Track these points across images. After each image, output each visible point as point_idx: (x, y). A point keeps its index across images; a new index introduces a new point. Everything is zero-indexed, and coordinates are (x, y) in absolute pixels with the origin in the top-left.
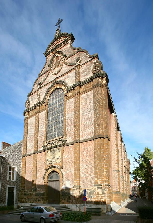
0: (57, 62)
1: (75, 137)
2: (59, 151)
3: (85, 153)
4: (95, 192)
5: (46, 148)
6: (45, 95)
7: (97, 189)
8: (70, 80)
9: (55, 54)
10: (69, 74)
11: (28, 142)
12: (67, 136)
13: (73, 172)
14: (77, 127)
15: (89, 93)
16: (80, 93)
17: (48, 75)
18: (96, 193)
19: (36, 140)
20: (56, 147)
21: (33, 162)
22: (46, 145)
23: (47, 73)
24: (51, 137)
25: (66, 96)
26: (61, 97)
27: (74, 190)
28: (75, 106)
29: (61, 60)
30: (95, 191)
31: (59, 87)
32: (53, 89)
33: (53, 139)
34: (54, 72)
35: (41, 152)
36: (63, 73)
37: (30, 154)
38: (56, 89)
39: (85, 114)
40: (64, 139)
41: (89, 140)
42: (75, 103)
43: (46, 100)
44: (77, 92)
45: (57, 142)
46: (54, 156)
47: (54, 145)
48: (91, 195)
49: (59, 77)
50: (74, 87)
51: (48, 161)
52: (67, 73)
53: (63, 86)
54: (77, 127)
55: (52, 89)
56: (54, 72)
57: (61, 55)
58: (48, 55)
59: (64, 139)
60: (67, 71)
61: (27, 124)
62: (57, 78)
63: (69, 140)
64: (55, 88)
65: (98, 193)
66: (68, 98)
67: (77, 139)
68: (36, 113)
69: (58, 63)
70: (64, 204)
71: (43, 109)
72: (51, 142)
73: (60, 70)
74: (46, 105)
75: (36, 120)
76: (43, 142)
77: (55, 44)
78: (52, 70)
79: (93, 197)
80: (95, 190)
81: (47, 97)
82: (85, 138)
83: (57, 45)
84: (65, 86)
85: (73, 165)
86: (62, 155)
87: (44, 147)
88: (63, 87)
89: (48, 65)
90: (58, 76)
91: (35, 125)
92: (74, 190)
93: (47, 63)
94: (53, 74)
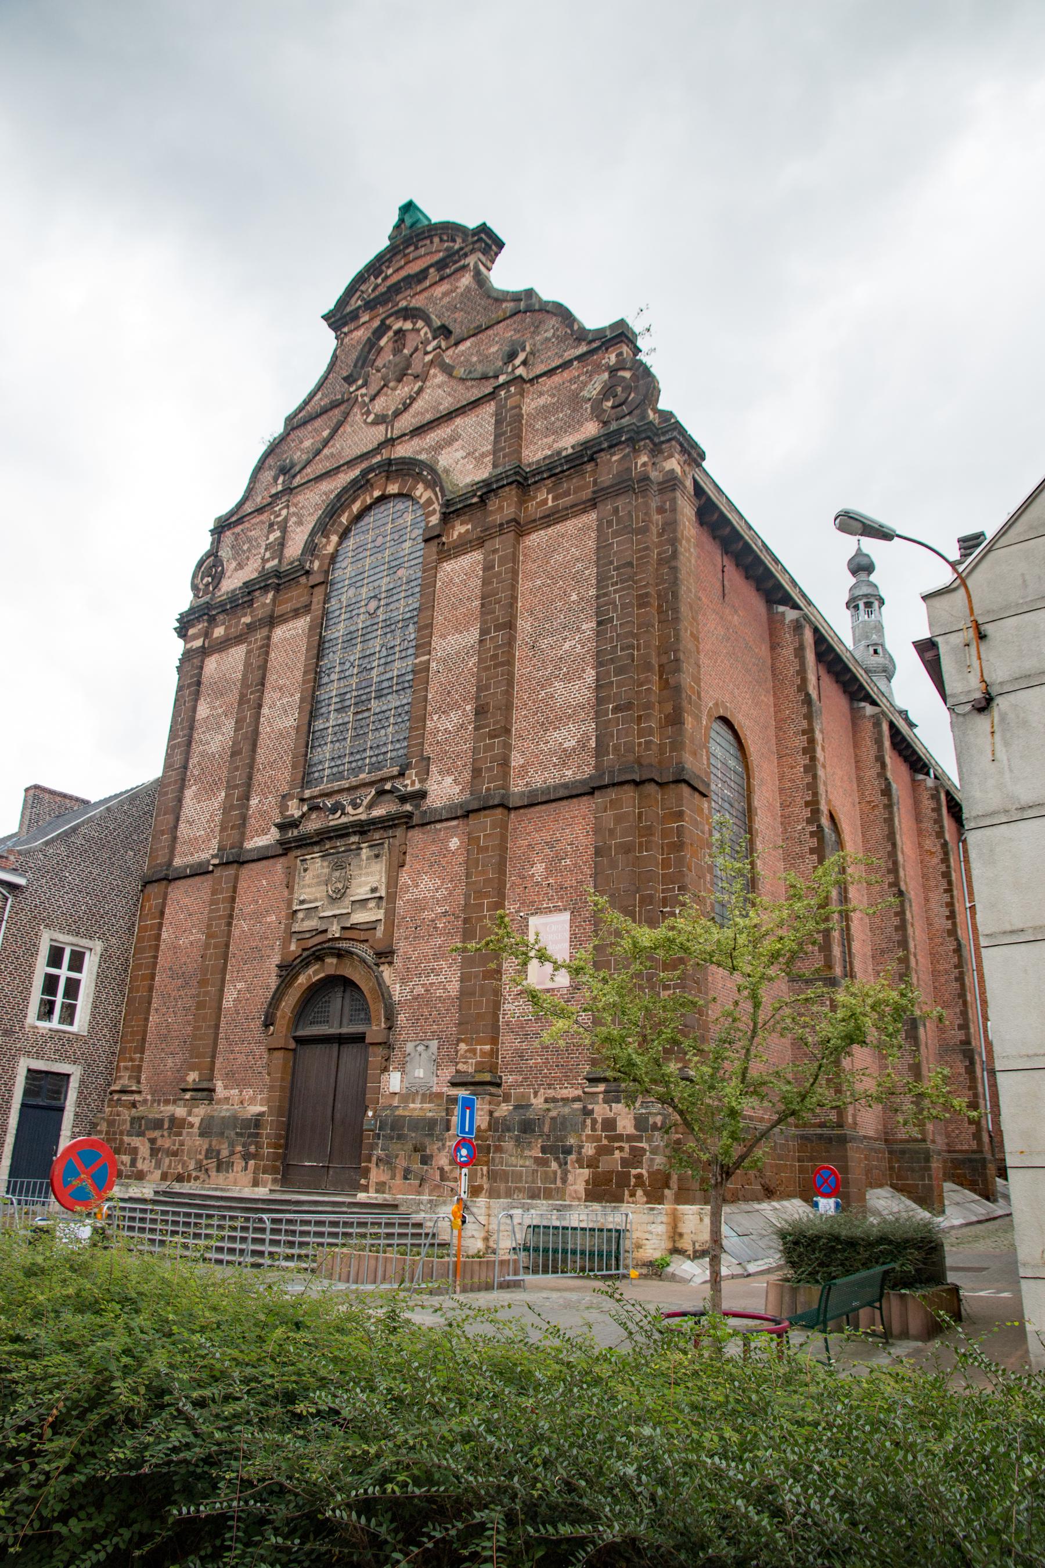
0: (397, 359)
1: (476, 772)
2: (377, 856)
3: (539, 869)
4: (594, 1121)
5: (296, 832)
6: (313, 534)
7: (605, 1102)
8: (461, 453)
9: (388, 322)
10: (458, 421)
11: (189, 793)
12: (433, 768)
13: (454, 987)
14: (493, 716)
15: (570, 526)
16: (520, 528)
17: (340, 424)
18: (599, 1126)
19: (236, 787)
21: (210, 919)
22: (297, 814)
23: (336, 411)
24: (335, 770)
25: (436, 541)
26: (408, 544)
28: (483, 598)
29: (416, 349)
30: (592, 1112)
31: (396, 491)
32: (365, 500)
33: (344, 784)
34: (379, 406)
35: (263, 856)
36: (429, 417)
37: (191, 866)
38: (383, 498)
39: (544, 643)
40: (413, 783)
42: (486, 582)
43: (317, 557)
44: (498, 518)
45: (365, 803)
46: (340, 886)
47: (344, 820)
48: (563, 1139)
49: (404, 435)
50: (487, 490)
51: (300, 915)
52: (449, 416)
53: (420, 487)
54: (493, 716)
55: (354, 501)
56: (379, 406)
57: (420, 324)
58: (345, 324)
59: (408, 782)
60: (447, 404)
61: (189, 686)
62: (390, 442)
63: (444, 789)
64: (377, 494)
65: (610, 1124)
66: (446, 553)
67: (488, 789)
68: (250, 628)
69: (402, 365)
71: (299, 605)
73: (413, 399)
74: (313, 587)
75: (247, 665)
76: (284, 797)
77: (390, 271)
78: (367, 399)
79: (573, 1157)
80: (590, 1107)
81: (324, 540)
82: (540, 779)
83: (403, 273)
84: (430, 485)
86: (392, 881)
87: (282, 827)
88: (421, 492)
89: (345, 374)
90: (396, 433)
91: (242, 696)
93: (339, 362)
94: (369, 420)
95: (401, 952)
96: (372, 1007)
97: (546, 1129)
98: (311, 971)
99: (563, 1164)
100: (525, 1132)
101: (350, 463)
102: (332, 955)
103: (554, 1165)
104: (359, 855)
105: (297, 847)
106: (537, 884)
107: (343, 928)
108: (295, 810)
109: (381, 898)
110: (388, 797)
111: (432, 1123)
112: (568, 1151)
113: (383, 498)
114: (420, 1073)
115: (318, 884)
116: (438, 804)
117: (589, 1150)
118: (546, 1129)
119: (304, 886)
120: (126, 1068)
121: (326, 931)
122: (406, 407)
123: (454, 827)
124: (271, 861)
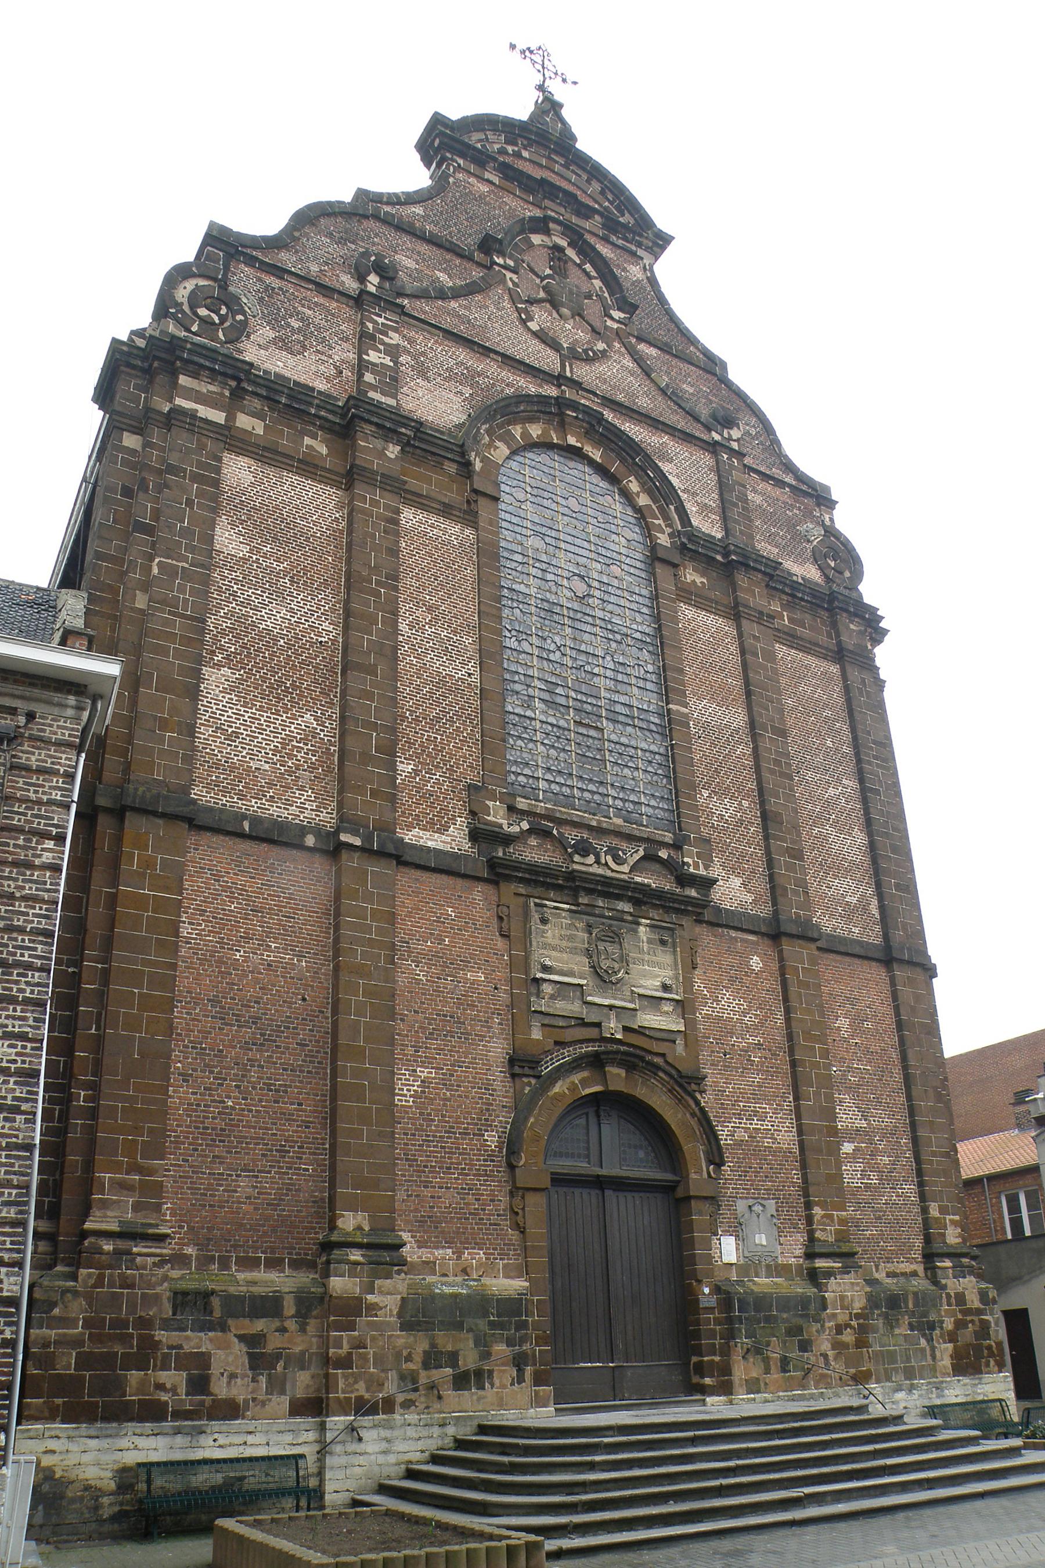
20: (637, 902)
27: (829, 1273)
36: (620, 397)
37: (255, 821)
41: (862, 952)
45: (631, 861)
64: (572, 440)
65: (960, 1299)
70: (758, 1392)
72: (572, 835)
79: (937, 1332)
85: (781, 1084)
87: (475, 835)
92: (829, 1273)
95: (709, 1081)
96: (687, 1147)
97: (911, 1306)
98: (576, 1078)
99: (930, 1340)
100: (892, 1309)
101: (509, 361)
102: (621, 1064)
103: (923, 1342)
104: (636, 931)
105: (521, 880)
106: (845, 1040)
107: (626, 1029)
108: (497, 815)
109: (677, 1001)
110: (657, 867)
111: (804, 1302)
112: (932, 1326)
113: (575, 453)
114: (761, 1239)
115: (573, 951)
116: (726, 905)
117: (949, 1324)
118: (911, 1306)
119: (545, 946)
120: (124, 1186)
121: (598, 1025)
122: (588, 360)
123: (753, 942)
124: (460, 882)
